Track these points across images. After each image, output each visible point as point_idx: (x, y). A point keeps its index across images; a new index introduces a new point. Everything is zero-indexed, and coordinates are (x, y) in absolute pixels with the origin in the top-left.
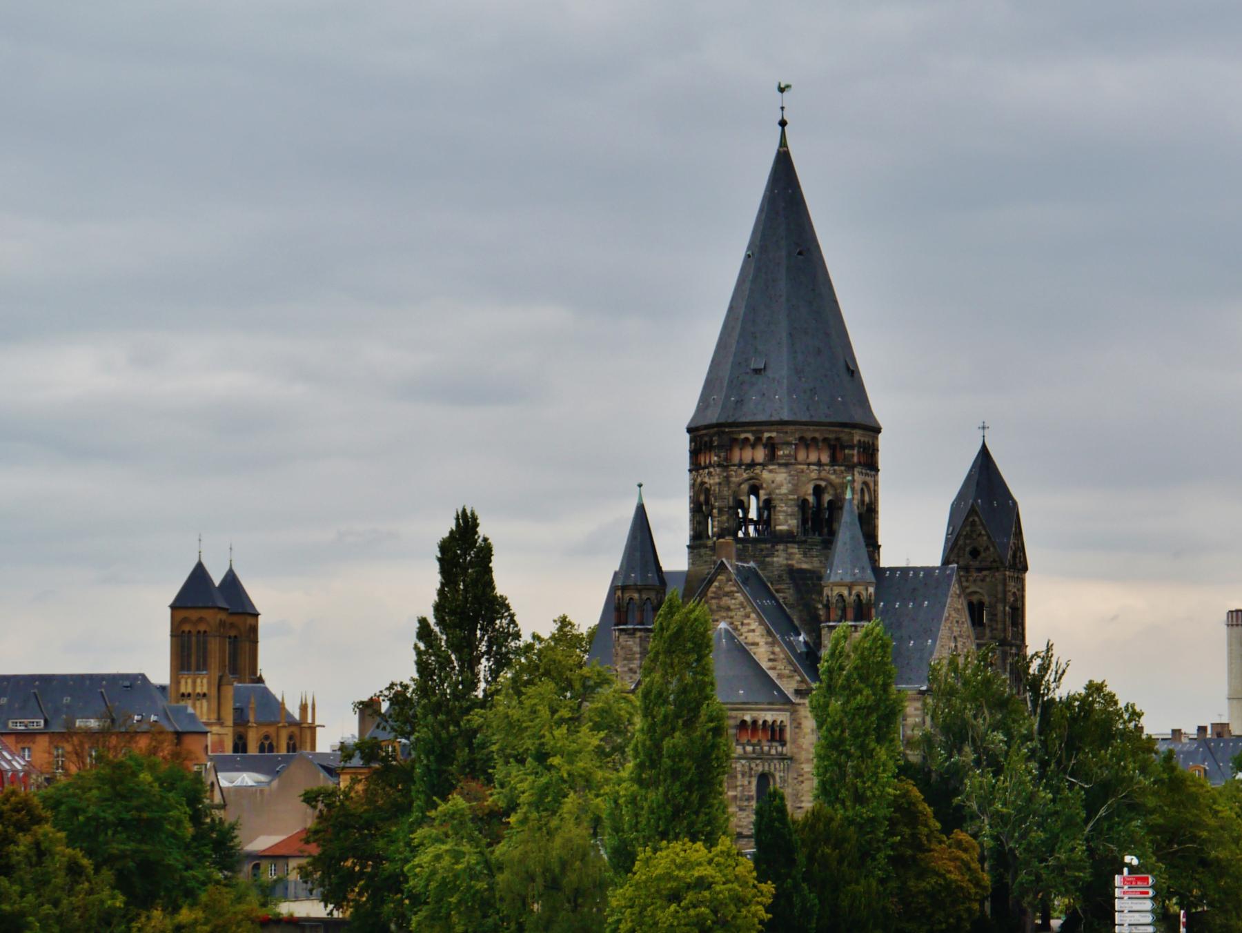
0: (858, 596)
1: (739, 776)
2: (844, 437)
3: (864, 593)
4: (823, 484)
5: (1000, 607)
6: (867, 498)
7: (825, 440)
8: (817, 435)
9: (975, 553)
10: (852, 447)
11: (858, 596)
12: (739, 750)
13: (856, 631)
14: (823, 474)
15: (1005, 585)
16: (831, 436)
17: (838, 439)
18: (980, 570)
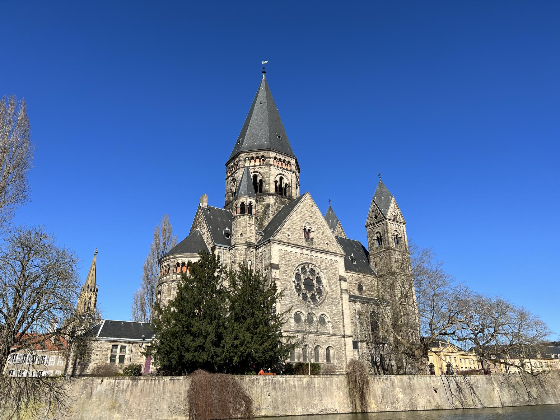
0: (243, 203)
1: (172, 290)
2: (266, 154)
3: (245, 201)
4: (257, 174)
5: (386, 235)
6: (285, 181)
7: (257, 158)
8: (253, 156)
9: (376, 217)
10: (270, 158)
11: (243, 203)
12: (174, 277)
13: (240, 218)
14: (256, 170)
15: (387, 225)
16: (260, 155)
17: (263, 156)
18: (377, 223)
